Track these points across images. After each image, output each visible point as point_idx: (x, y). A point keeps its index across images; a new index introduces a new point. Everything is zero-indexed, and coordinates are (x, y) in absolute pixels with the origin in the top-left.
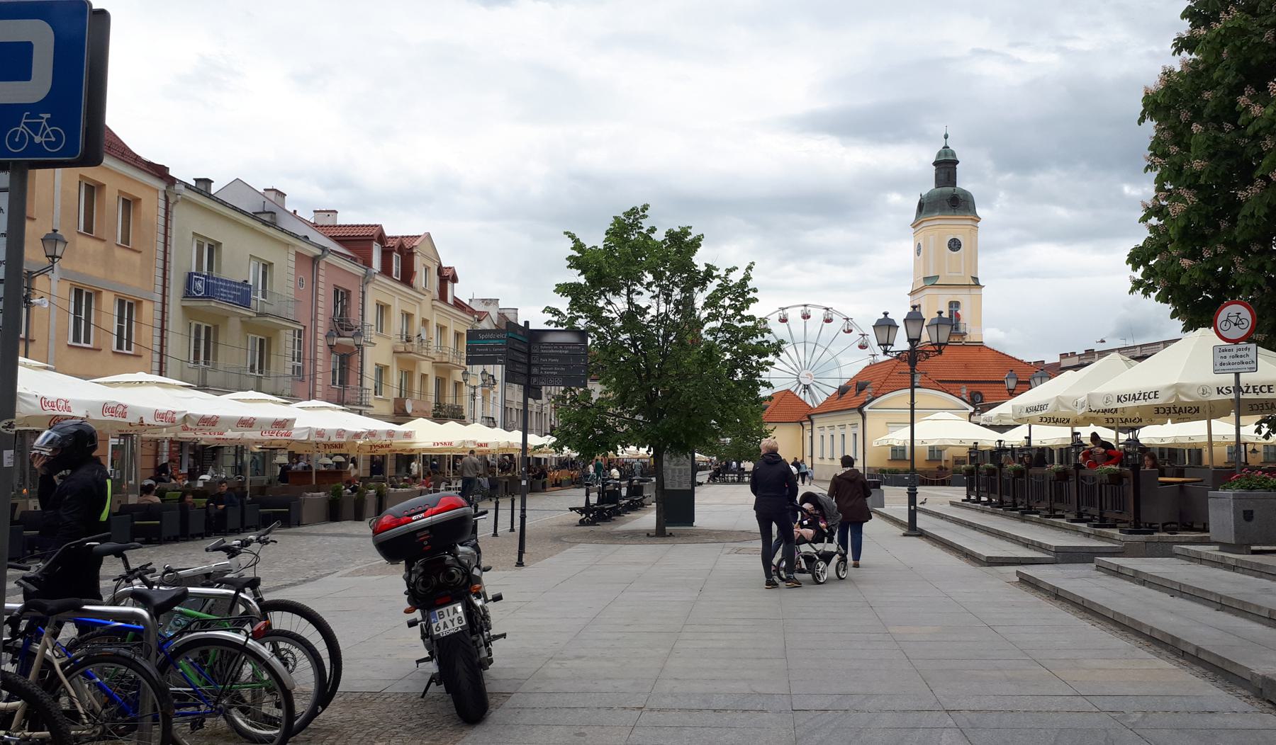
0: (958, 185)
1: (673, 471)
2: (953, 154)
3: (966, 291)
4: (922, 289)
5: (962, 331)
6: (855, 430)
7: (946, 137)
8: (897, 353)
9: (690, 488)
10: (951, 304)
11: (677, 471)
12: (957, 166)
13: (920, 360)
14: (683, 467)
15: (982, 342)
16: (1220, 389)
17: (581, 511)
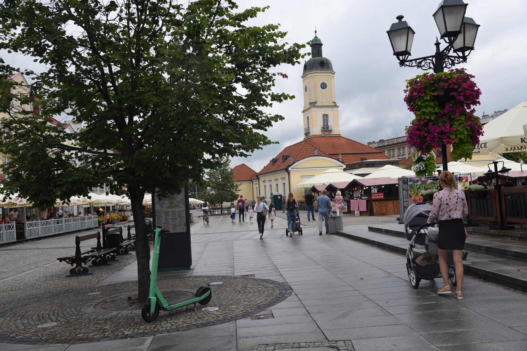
0: (323, 56)
1: (167, 213)
2: (320, 40)
3: (330, 109)
4: (309, 109)
5: (330, 129)
6: (284, 181)
7: (316, 32)
8: (418, 61)
9: (185, 231)
10: (324, 115)
11: (171, 214)
12: (322, 47)
13: (446, 67)
14: (176, 209)
15: (340, 135)
16: (523, 139)
17: (71, 260)
